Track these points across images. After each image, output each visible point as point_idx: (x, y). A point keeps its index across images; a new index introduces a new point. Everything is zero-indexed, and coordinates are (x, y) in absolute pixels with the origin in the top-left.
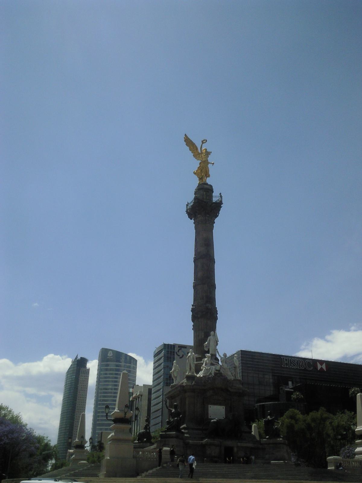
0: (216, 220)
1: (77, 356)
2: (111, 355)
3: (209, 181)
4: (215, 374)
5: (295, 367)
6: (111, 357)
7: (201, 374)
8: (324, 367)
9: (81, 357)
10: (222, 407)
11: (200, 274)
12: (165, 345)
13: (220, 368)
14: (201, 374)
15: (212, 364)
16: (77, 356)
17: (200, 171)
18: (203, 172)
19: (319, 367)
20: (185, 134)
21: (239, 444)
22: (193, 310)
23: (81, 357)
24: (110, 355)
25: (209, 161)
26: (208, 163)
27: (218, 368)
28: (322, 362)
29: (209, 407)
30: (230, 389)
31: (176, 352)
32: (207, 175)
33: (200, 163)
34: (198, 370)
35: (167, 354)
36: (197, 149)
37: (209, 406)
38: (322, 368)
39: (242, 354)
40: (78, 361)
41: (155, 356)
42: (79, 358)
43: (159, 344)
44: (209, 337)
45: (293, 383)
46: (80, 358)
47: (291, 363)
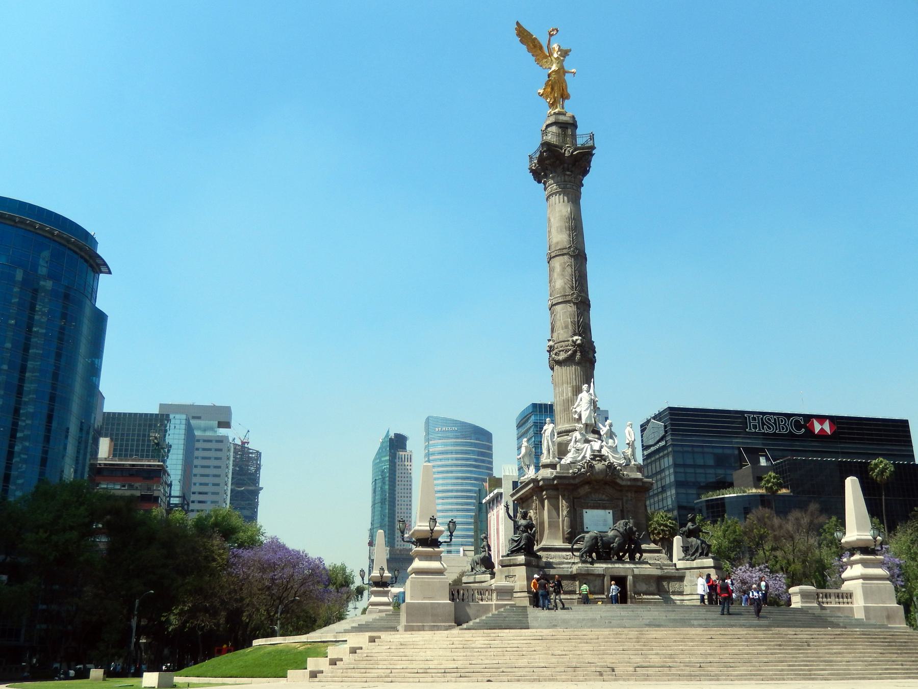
0: (586, 180)
3: (571, 108)
4: (594, 457)
5: (770, 431)
7: (567, 460)
8: (827, 427)
10: (608, 511)
11: (559, 283)
12: (534, 405)
13: (602, 447)
14: (567, 460)
15: (587, 441)
17: (549, 90)
19: (817, 427)
20: (517, 23)
21: (636, 572)
22: (551, 349)
25: (566, 69)
26: (565, 72)
27: (596, 445)
28: (821, 418)
29: (585, 514)
30: (619, 481)
32: (564, 96)
33: (549, 76)
36: (541, 48)
37: (584, 511)
38: (822, 430)
39: (671, 414)
40: (391, 439)
41: (519, 426)
42: (392, 435)
43: (524, 404)
44: (580, 396)
45: (768, 459)
47: (763, 424)
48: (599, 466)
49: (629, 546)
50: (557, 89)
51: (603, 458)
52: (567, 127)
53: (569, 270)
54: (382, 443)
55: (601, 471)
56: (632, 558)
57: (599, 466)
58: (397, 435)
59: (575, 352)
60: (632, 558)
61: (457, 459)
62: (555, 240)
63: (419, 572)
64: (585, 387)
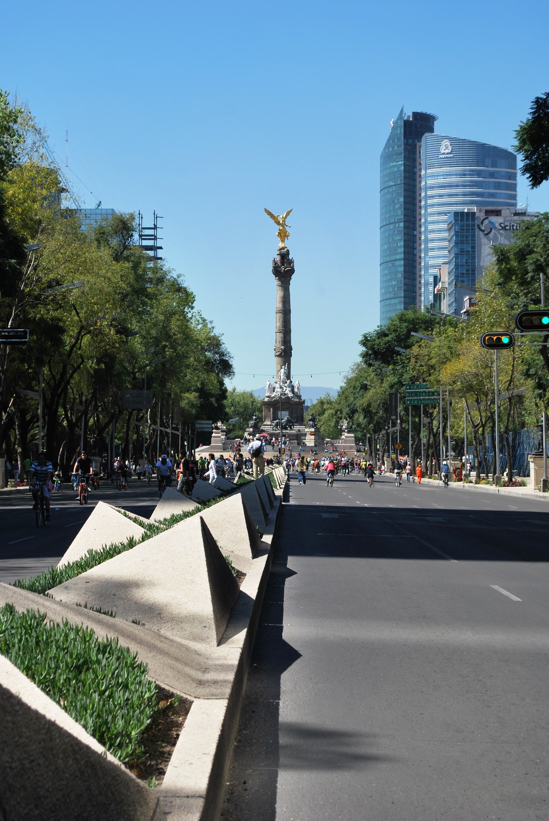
0: (293, 277)
1: (402, 111)
2: (450, 151)
6: (448, 154)
9: (414, 113)
11: (278, 324)
15: (281, 388)
16: (402, 111)
18: (283, 235)
22: (275, 350)
23: (414, 113)
24: (447, 151)
31: (478, 226)
34: (274, 391)
35: (461, 229)
42: (408, 114)
46: (411, 115)
48: (283, 397)
49: (290, 424)
50: (283, 235)
51: (285, 394)
52: (284, 256)
53: (281, 319)
54: (394, 128)
55: (284, 399)
56: (291, 428)
57: (283, 397)
58: (416, 115)
59: (282, 353)
60: (291, 428)
61: (464, 195)
62: (278, 306)
63: (214, 437)
64: (283, 367)
